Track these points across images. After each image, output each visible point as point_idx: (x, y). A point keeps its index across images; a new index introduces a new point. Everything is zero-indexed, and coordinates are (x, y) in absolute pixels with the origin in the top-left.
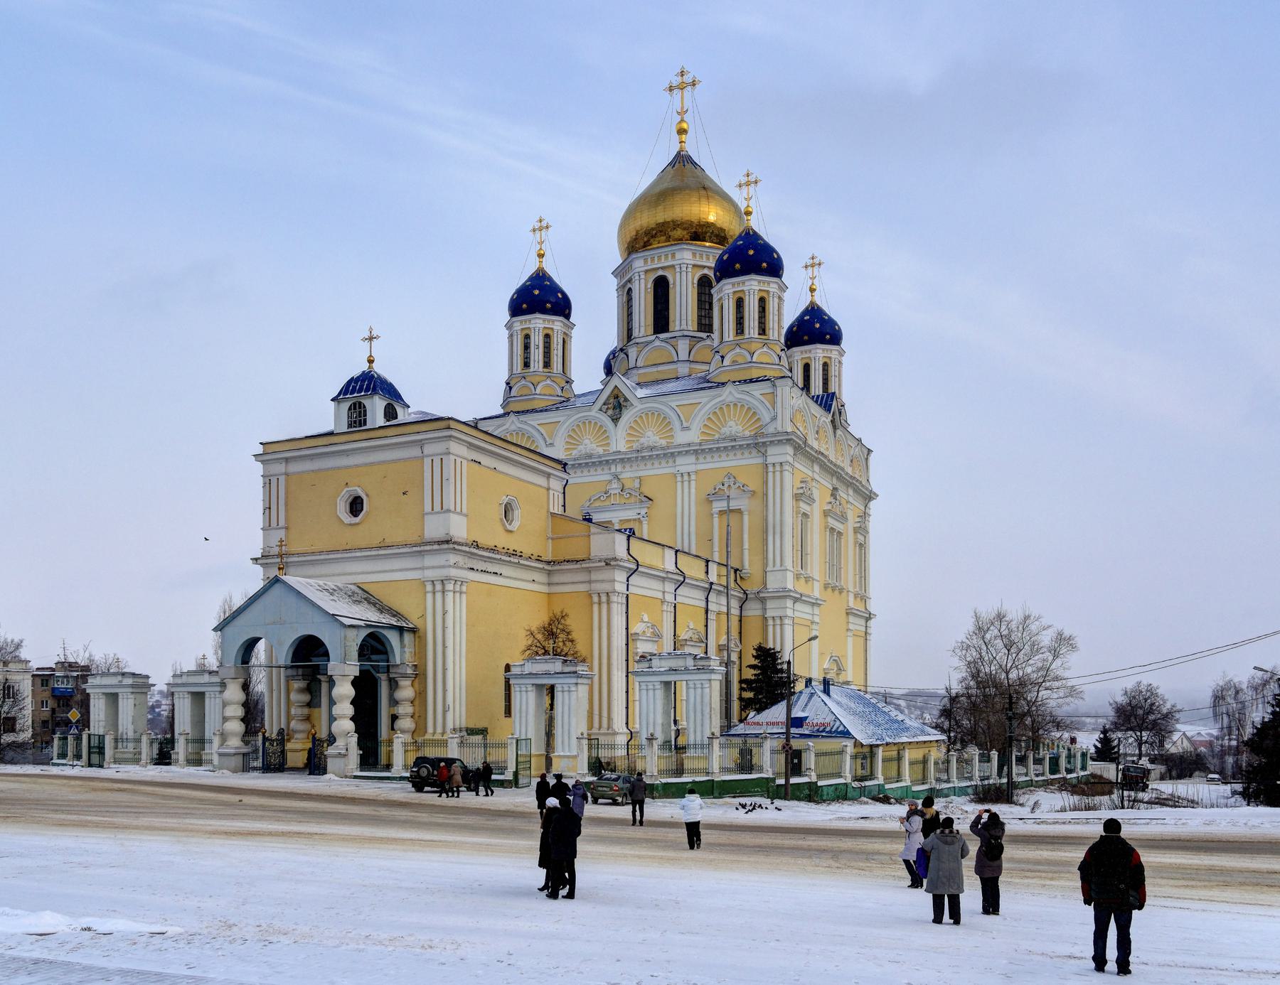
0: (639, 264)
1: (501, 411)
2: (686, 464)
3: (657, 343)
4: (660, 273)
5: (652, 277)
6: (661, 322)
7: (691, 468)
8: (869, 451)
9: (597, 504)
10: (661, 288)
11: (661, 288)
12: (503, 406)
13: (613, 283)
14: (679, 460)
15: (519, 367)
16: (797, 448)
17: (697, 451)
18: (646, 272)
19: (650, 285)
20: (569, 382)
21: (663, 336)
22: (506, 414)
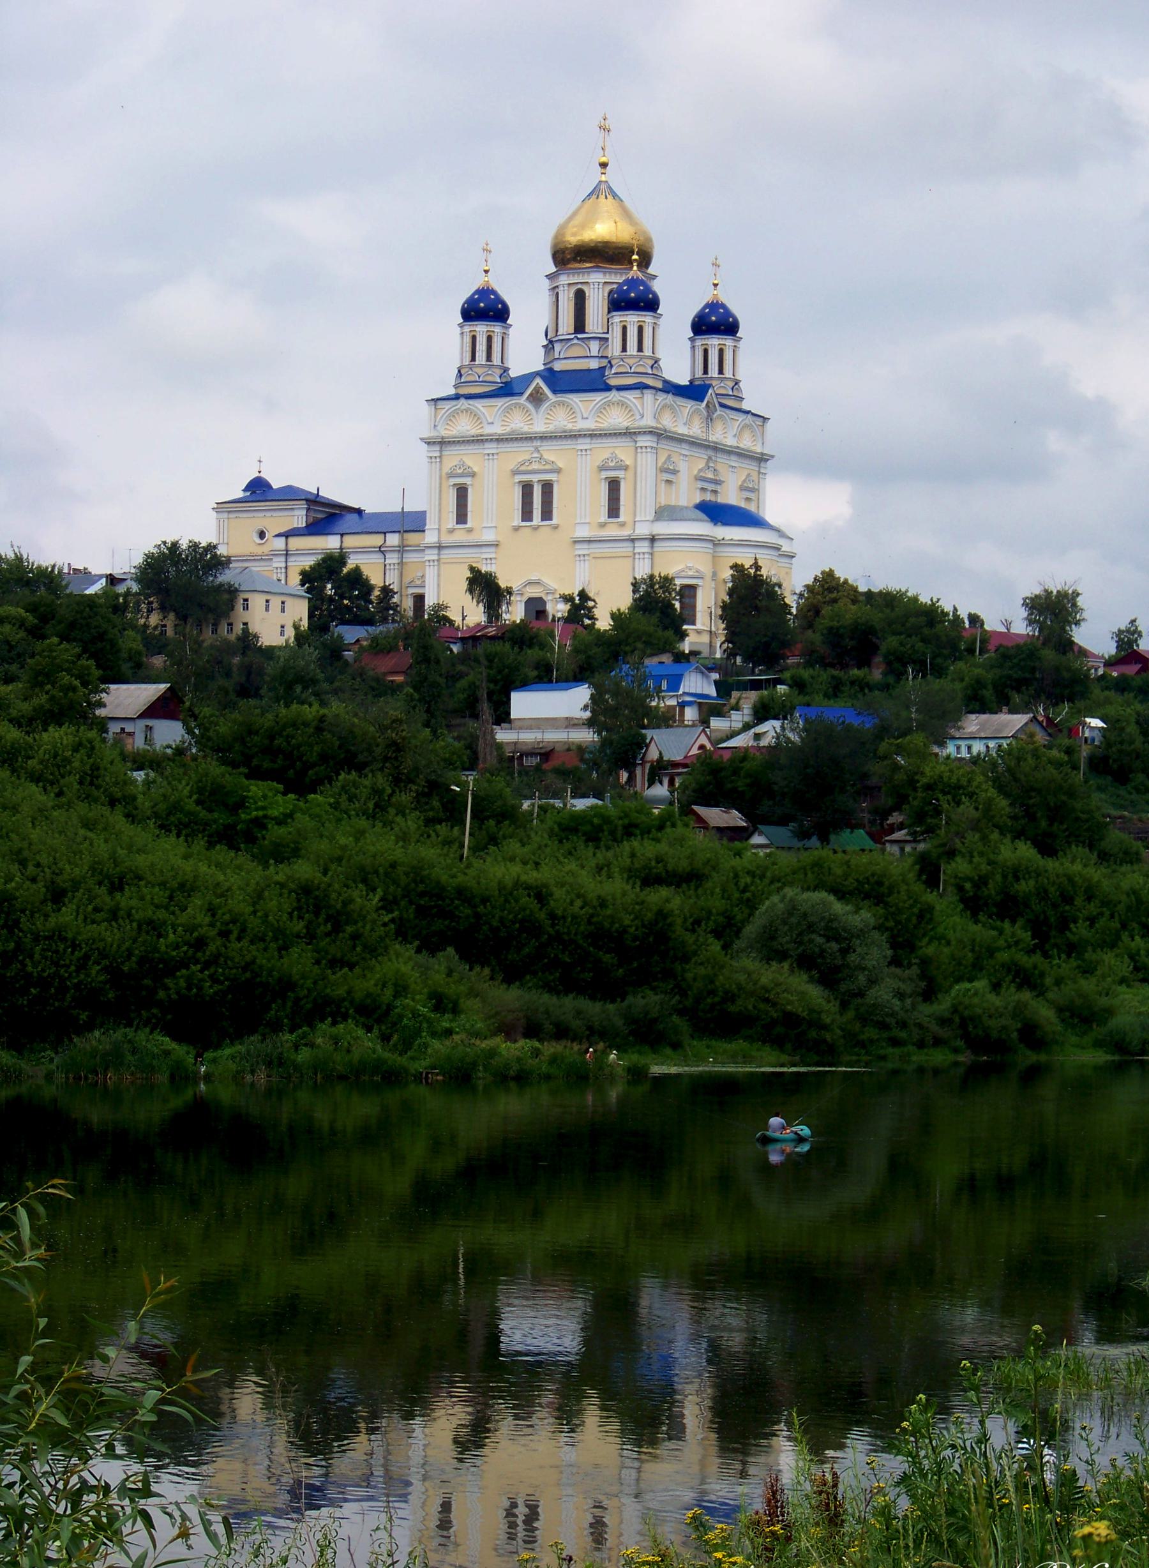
0: (564, 280)
1: (452, 391)
2: (584, 444)
3: (575, 341)
4: (580, 286)
5: (574, 289)
6: (580, 325)
7: (588, 447)
8: (765, 419)
9: (523, 468)
10: (580, 298)
11: (580, 298)
12: (456, 386)
13: (547, 284)
14: (580, 441)
15: (467, 361)
16: (659, 435)
17: (593, 435)
18: (570, 284)
19: (572, 295)
20: (506, 370)
21: (579, 336)
22: (457, 397)
